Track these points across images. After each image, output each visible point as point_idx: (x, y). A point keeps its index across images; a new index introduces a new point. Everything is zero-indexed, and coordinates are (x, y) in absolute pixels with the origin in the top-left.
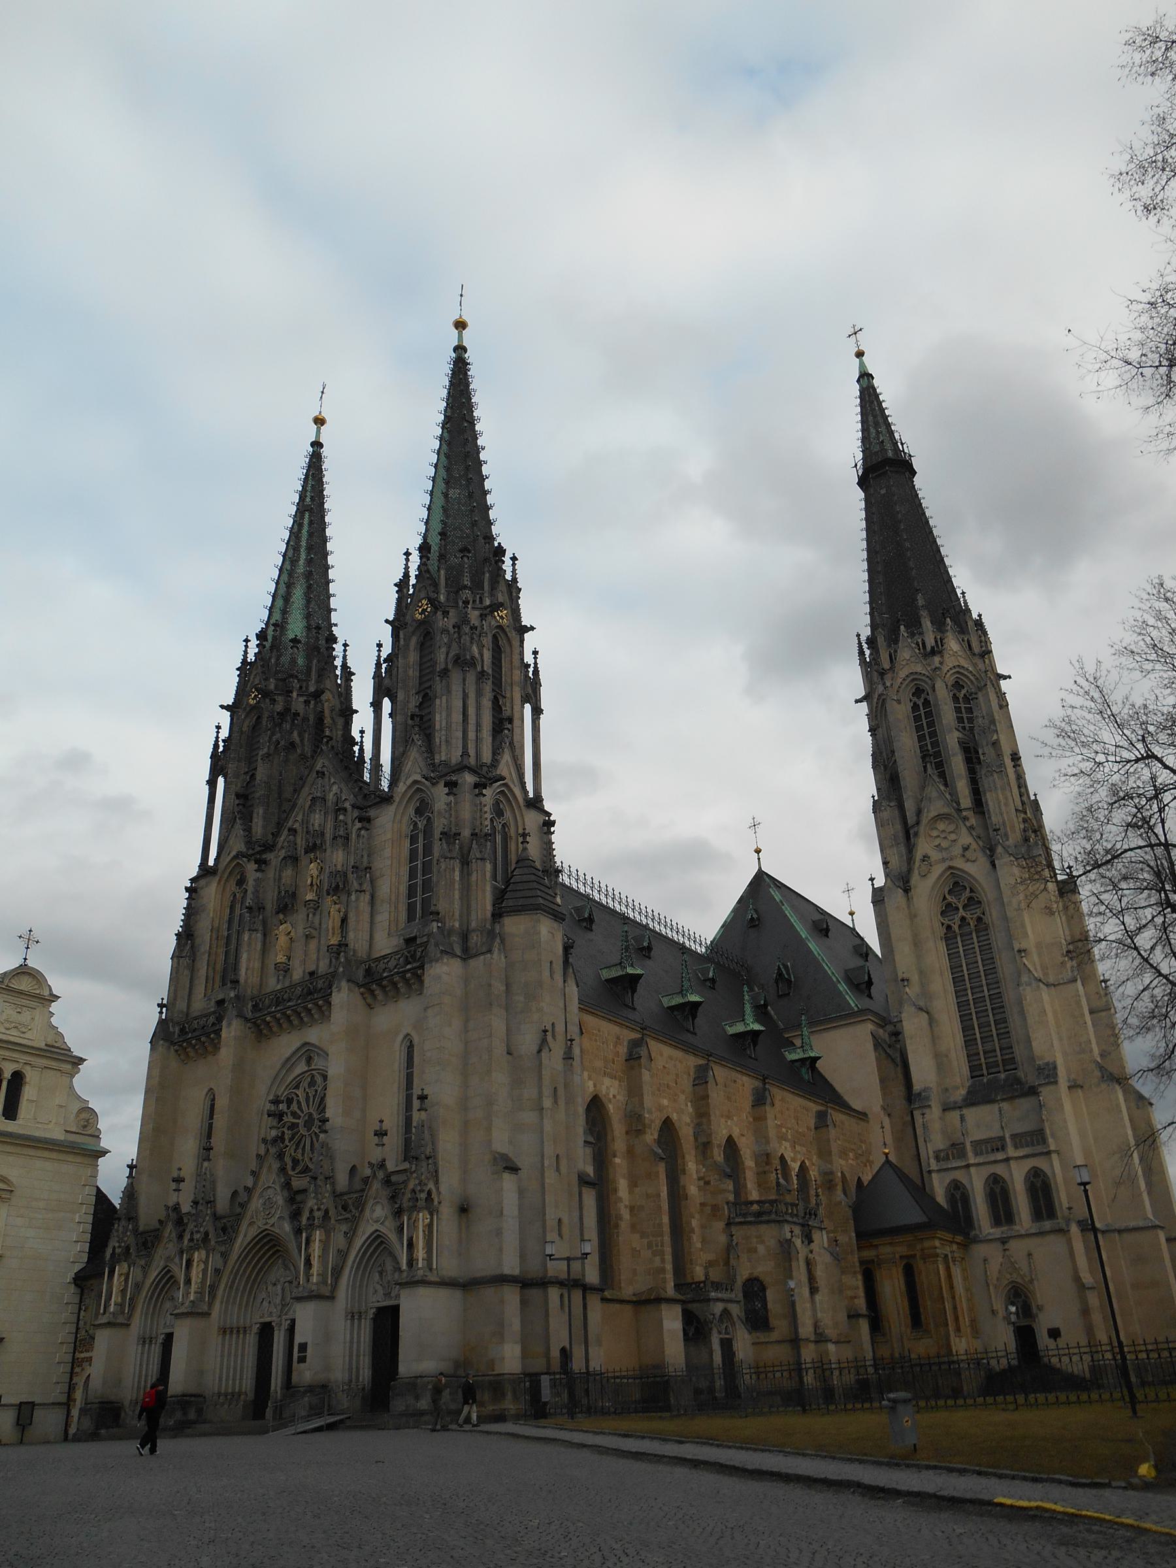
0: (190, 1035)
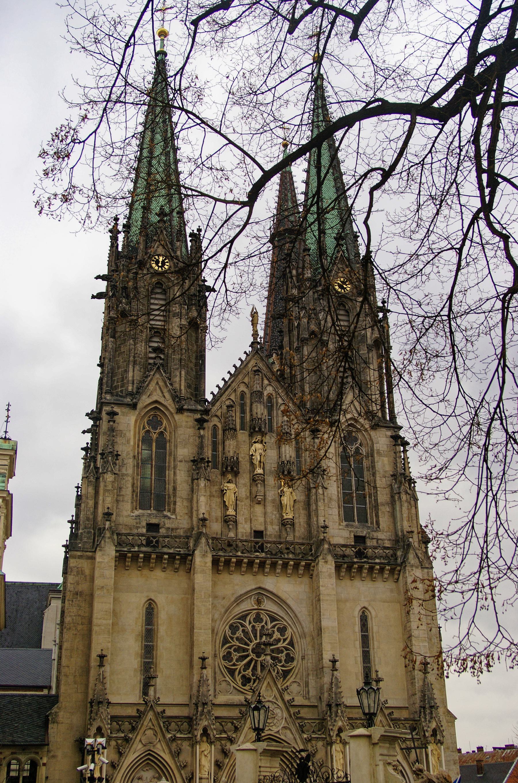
0: (136, 549)
